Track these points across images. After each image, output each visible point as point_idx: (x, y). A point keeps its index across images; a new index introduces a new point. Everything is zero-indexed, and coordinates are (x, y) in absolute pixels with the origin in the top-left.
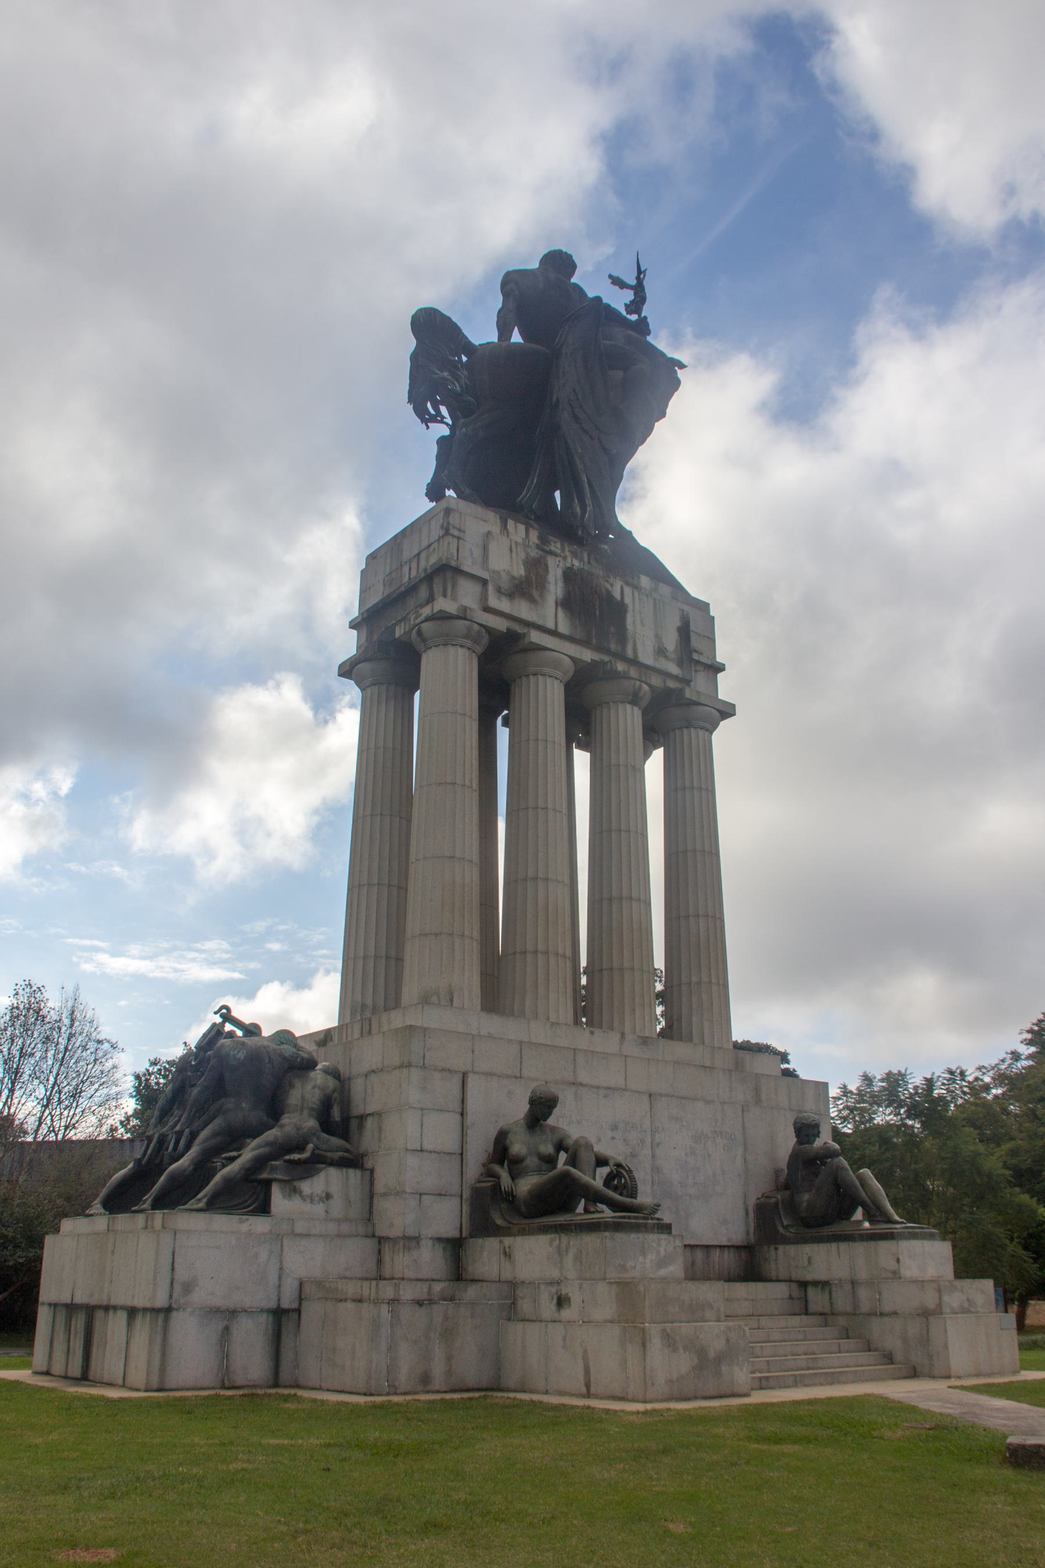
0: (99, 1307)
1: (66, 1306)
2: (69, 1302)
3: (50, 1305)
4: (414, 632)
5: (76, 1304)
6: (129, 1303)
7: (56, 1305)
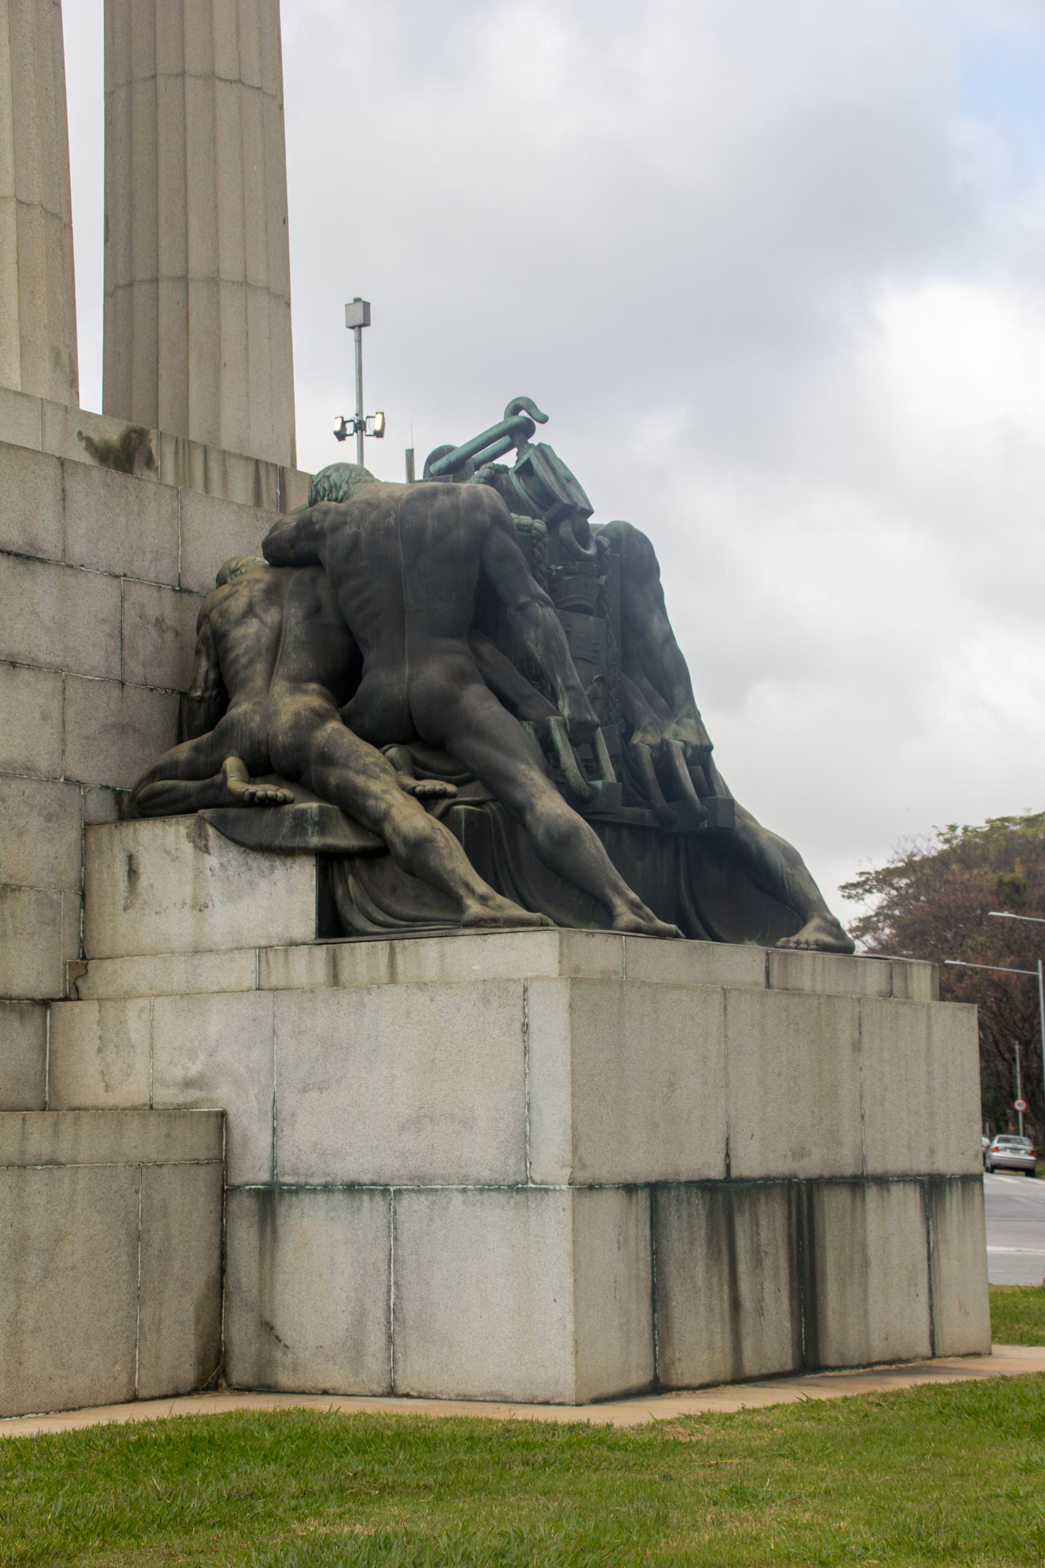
0: (833, 1181)
1: (706, 1186)
2: (717, 1172)
3: (629, 1188)
5: (741, 1180)
6: (922, 1166)
7: (656, 1189)
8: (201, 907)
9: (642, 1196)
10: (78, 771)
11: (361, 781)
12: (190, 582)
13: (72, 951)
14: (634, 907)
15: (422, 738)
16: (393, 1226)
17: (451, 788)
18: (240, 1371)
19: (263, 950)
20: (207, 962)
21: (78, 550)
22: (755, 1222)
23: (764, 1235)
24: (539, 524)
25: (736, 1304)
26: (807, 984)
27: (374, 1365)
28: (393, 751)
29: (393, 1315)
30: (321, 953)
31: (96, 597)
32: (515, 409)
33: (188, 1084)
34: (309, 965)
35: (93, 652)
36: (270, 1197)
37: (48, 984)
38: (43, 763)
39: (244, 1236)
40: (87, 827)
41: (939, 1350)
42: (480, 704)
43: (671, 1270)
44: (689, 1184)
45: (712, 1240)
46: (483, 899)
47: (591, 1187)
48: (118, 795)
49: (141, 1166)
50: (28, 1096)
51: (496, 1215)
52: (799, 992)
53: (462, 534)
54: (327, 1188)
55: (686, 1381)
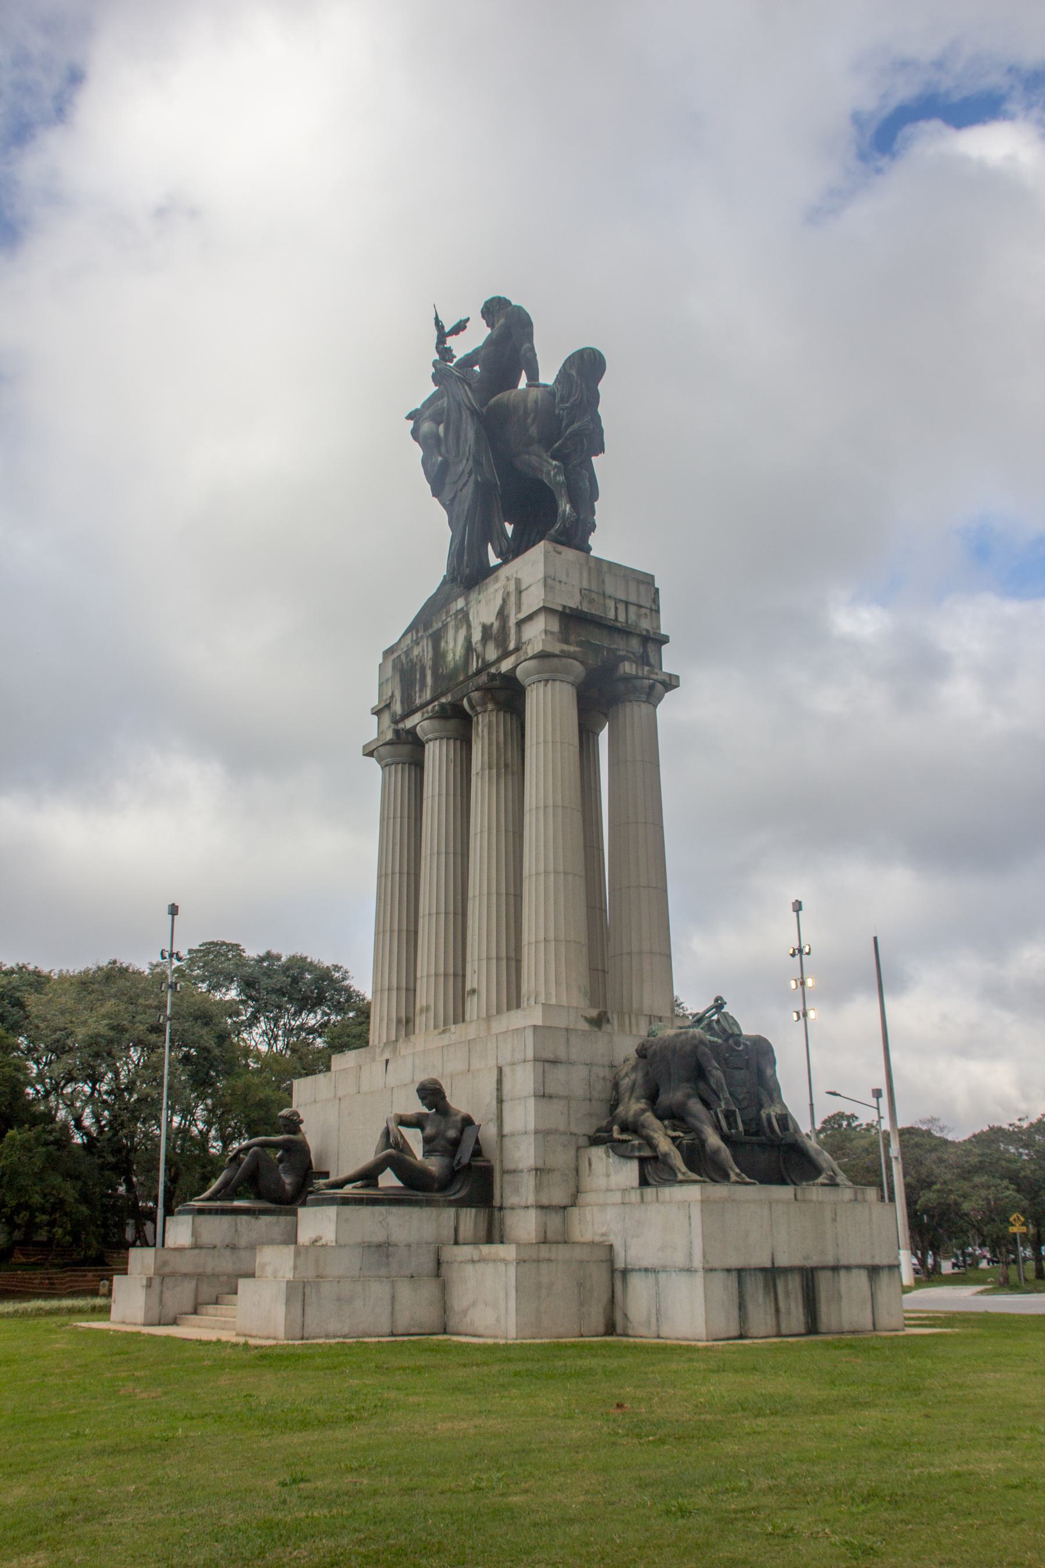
0: (823, 1268)
1: (763, 1270)
3: (729, 1270)
4: (646, 682)
5: (779, 1268)
6: (868, 1261)
7: (740, 1271)
8: (608, 1176)
9: (734, 1274)
10: (574, 1130)
11: (652, 1133)
12: (616, 1063)
13: (574, 1190)
14: (737, 1175)
15: (675, 1117)
16: (657, 1283)
17: (682, 1135)
18: (619, 1330)
19: (624, 1190)
20: (609, 1194)
21: (573, 1057)
22: (786, 1282)
23: (790, 1286)
24: (720, 1041)
25: (777, 1310)
26: (814, 1198)
27: (654, 1328)
28: (666, 1122)
29: (658, 1311)
30: (638, 1191)
31: (580, 1073)
32: (716, 1000)
33: (603, 1235)
34: (634, 1196)
35: (579, 1089)
36: (625, 1272)
37: (564, 1202)
38: (562, 1127)
39: (618, 1284)
40: (578, 1148)
41: (878, 1327)
42: (695, 1106)
43: (747, 1298)
44: (755, 1269)
45: (766, 1286)
46: (684, 1174)
47: (711, 1270)
48: (589, 1137)
49: (582, 1262)
50: (560, 1238)
51: (683, 1279)
52: (811, 1201)
53: (688, 1048)
54: (640, 1270)
55: (755, 1335)
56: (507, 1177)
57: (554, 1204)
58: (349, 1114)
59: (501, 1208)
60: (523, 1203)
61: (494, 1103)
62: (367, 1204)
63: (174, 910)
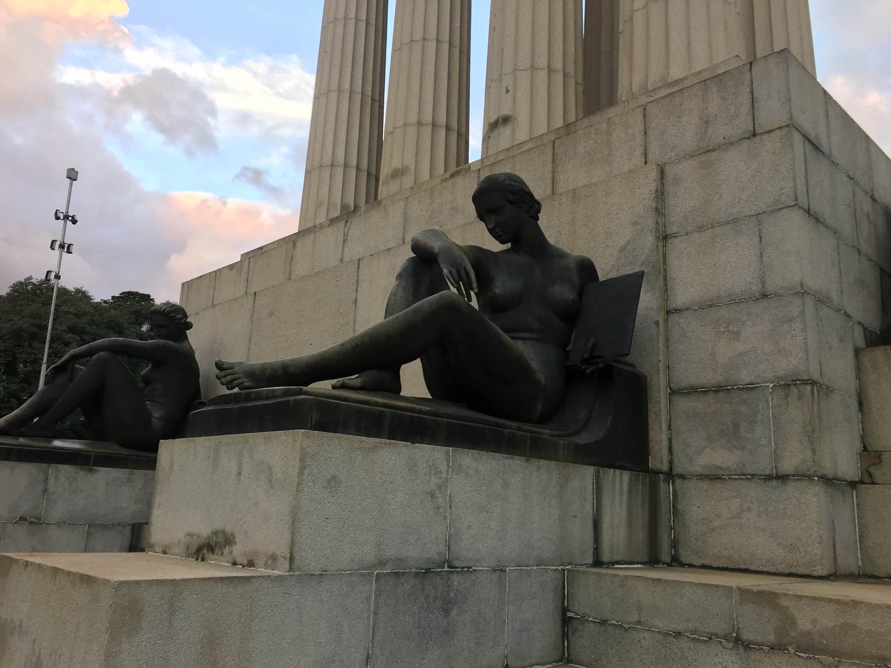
56: (683, 404)
57: (840, 474)
58: (271, 314)
59: (670, 476)
60: (764, 465)
61: (649, 240)
62: (393, 435)
63: (72, 175)
